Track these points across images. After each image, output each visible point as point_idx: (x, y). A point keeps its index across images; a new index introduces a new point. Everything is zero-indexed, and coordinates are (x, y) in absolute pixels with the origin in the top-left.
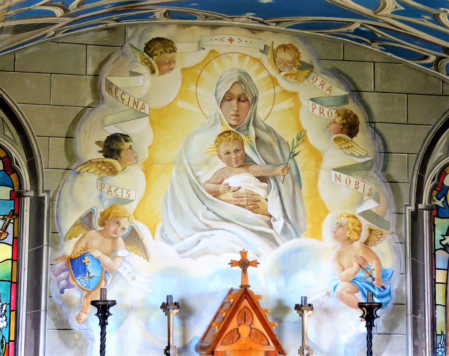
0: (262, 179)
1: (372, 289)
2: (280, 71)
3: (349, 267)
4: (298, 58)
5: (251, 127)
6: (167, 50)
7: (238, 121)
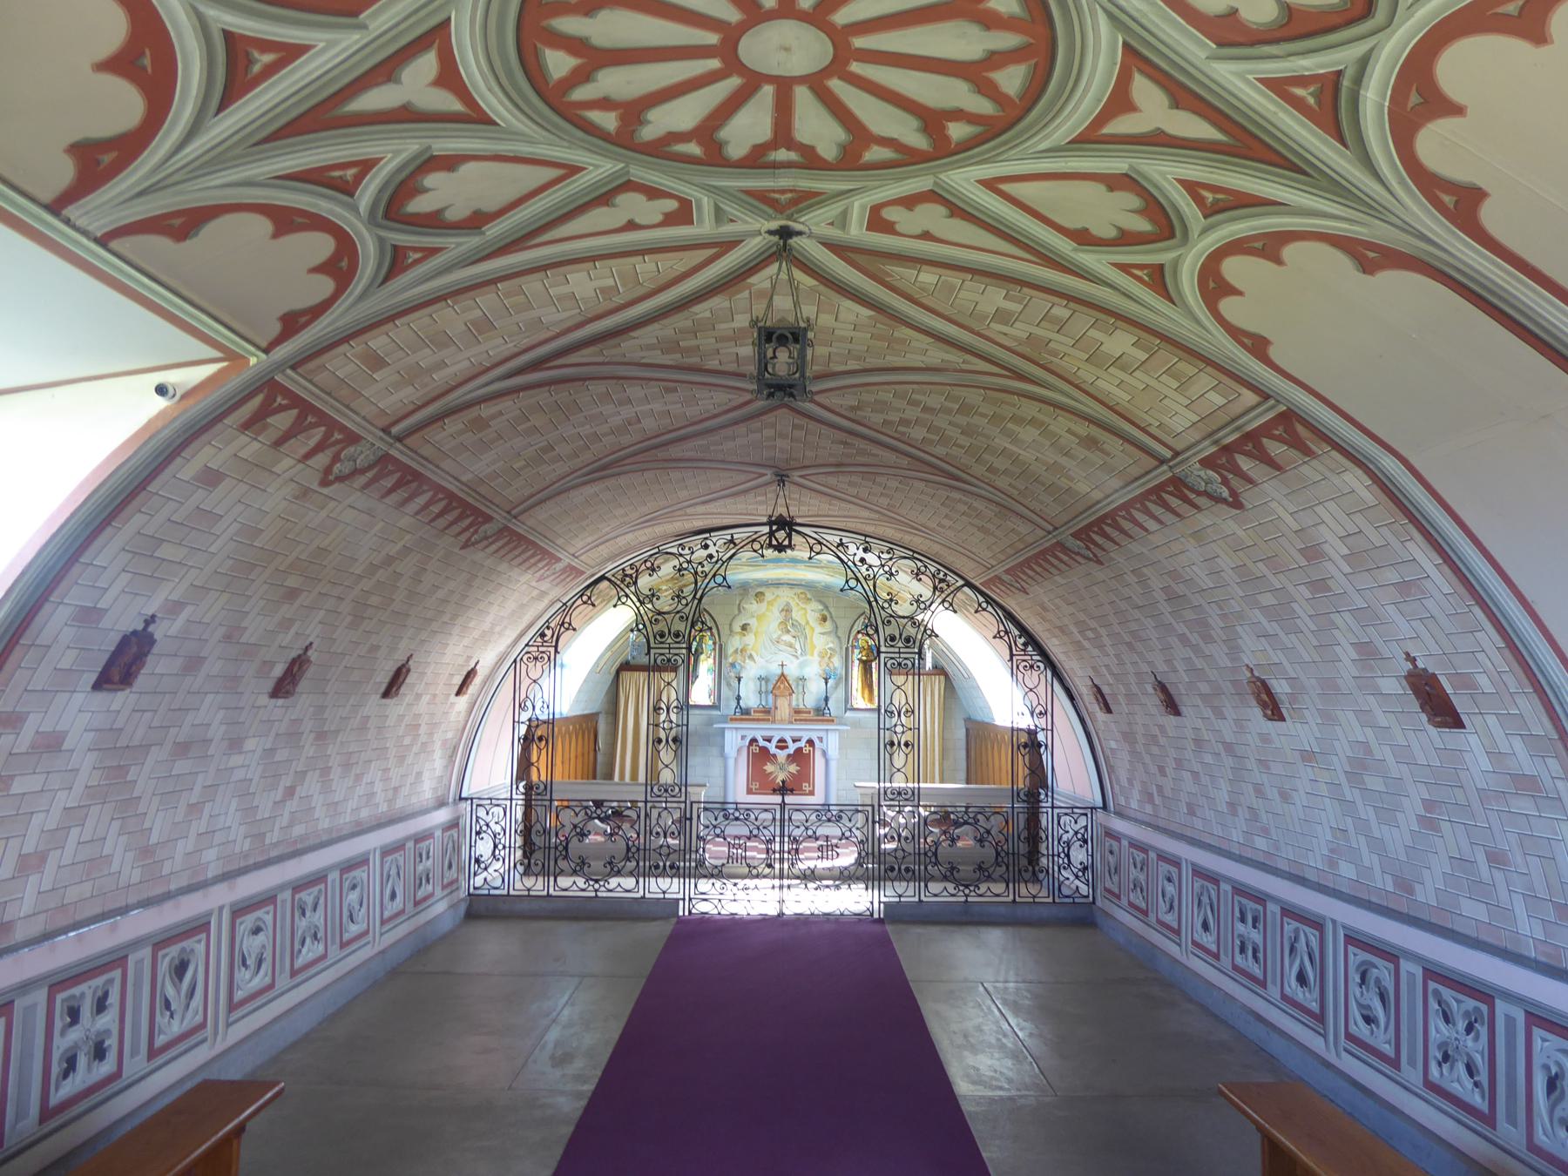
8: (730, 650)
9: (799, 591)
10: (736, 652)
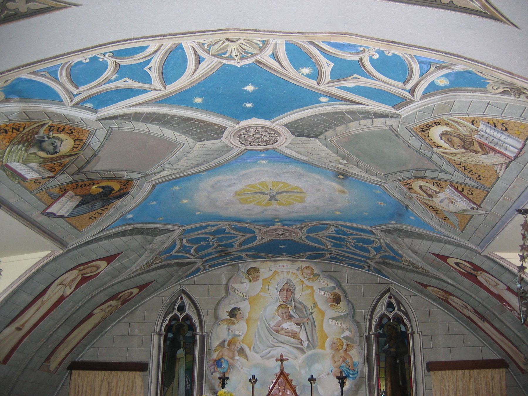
0: (298, 324)
1: (349, 371)
2: (305, 278)
3: (338, 362)
4: (313, 271)
5: (293, 302)
6: (256, 272)
7: (287, 299)
8: (215, 343)
9: (303, 265)
10: (222, 344)
